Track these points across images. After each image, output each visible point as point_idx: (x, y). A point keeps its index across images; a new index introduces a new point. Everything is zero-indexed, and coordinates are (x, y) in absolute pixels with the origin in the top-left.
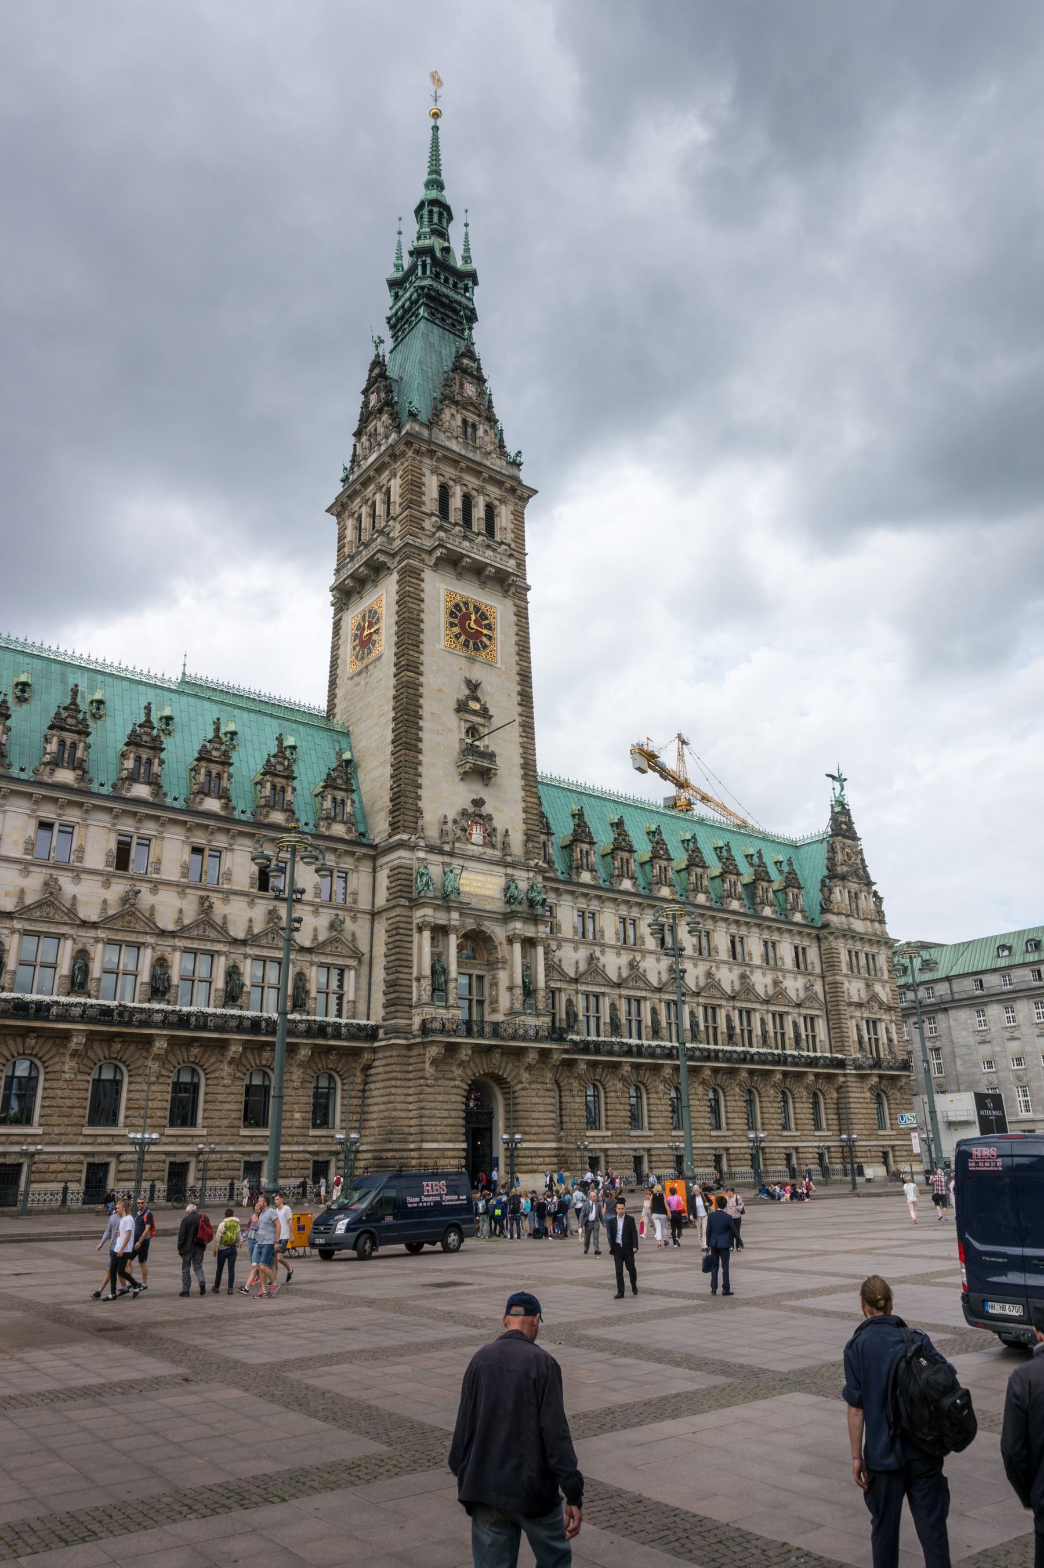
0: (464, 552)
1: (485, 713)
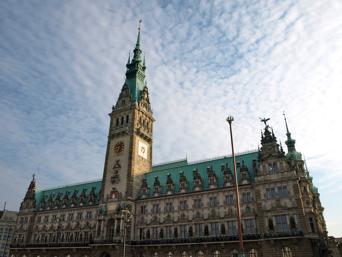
0: (114, 133)
1: (120, 166)
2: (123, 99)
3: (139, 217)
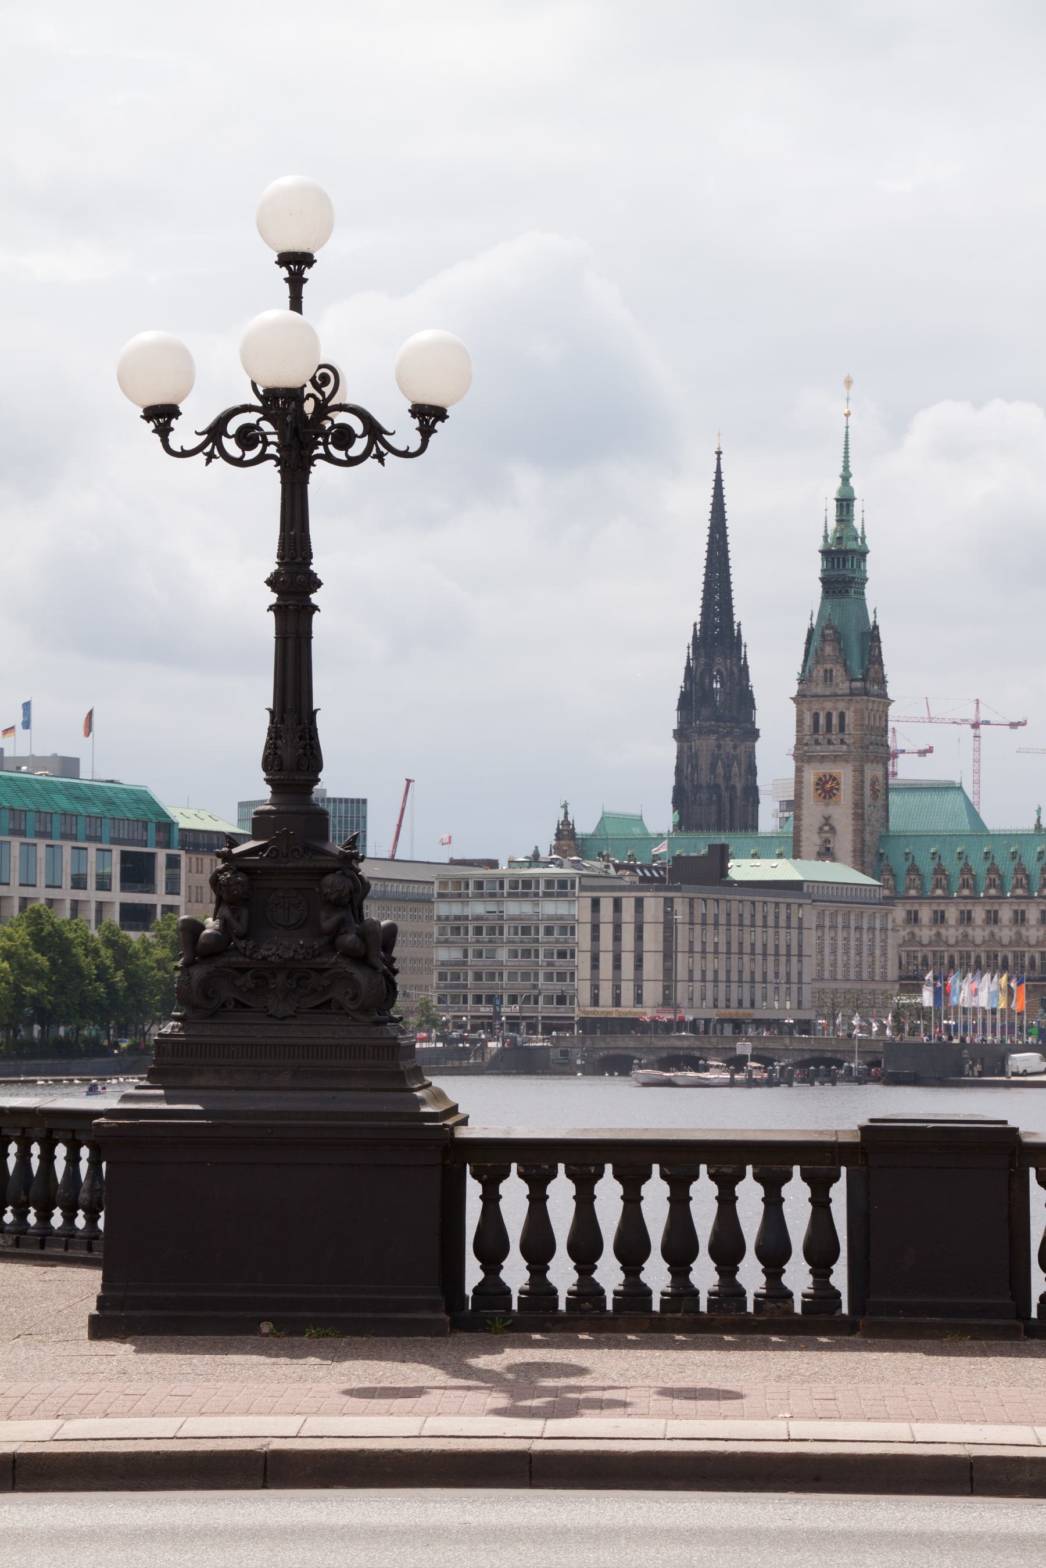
1: (833, 830)
2: (828, 666)
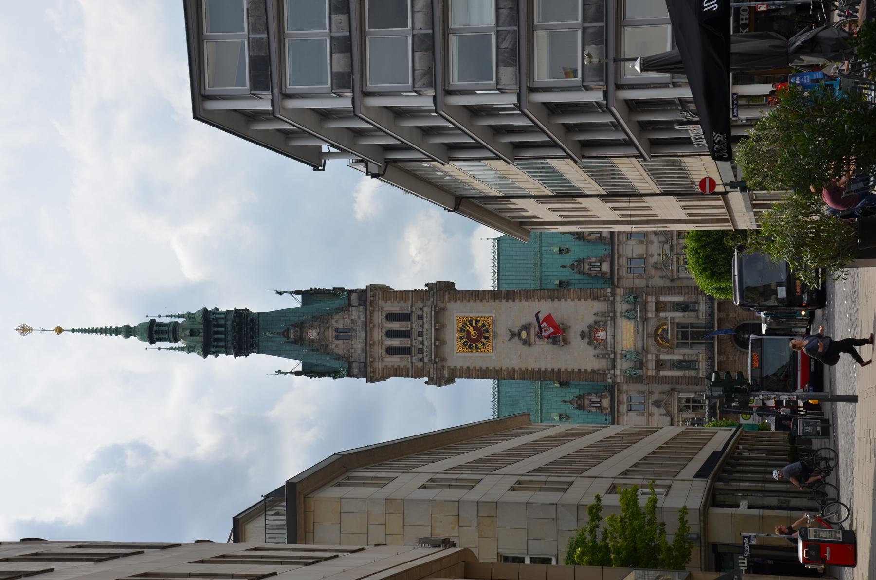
3: (652, 277)
